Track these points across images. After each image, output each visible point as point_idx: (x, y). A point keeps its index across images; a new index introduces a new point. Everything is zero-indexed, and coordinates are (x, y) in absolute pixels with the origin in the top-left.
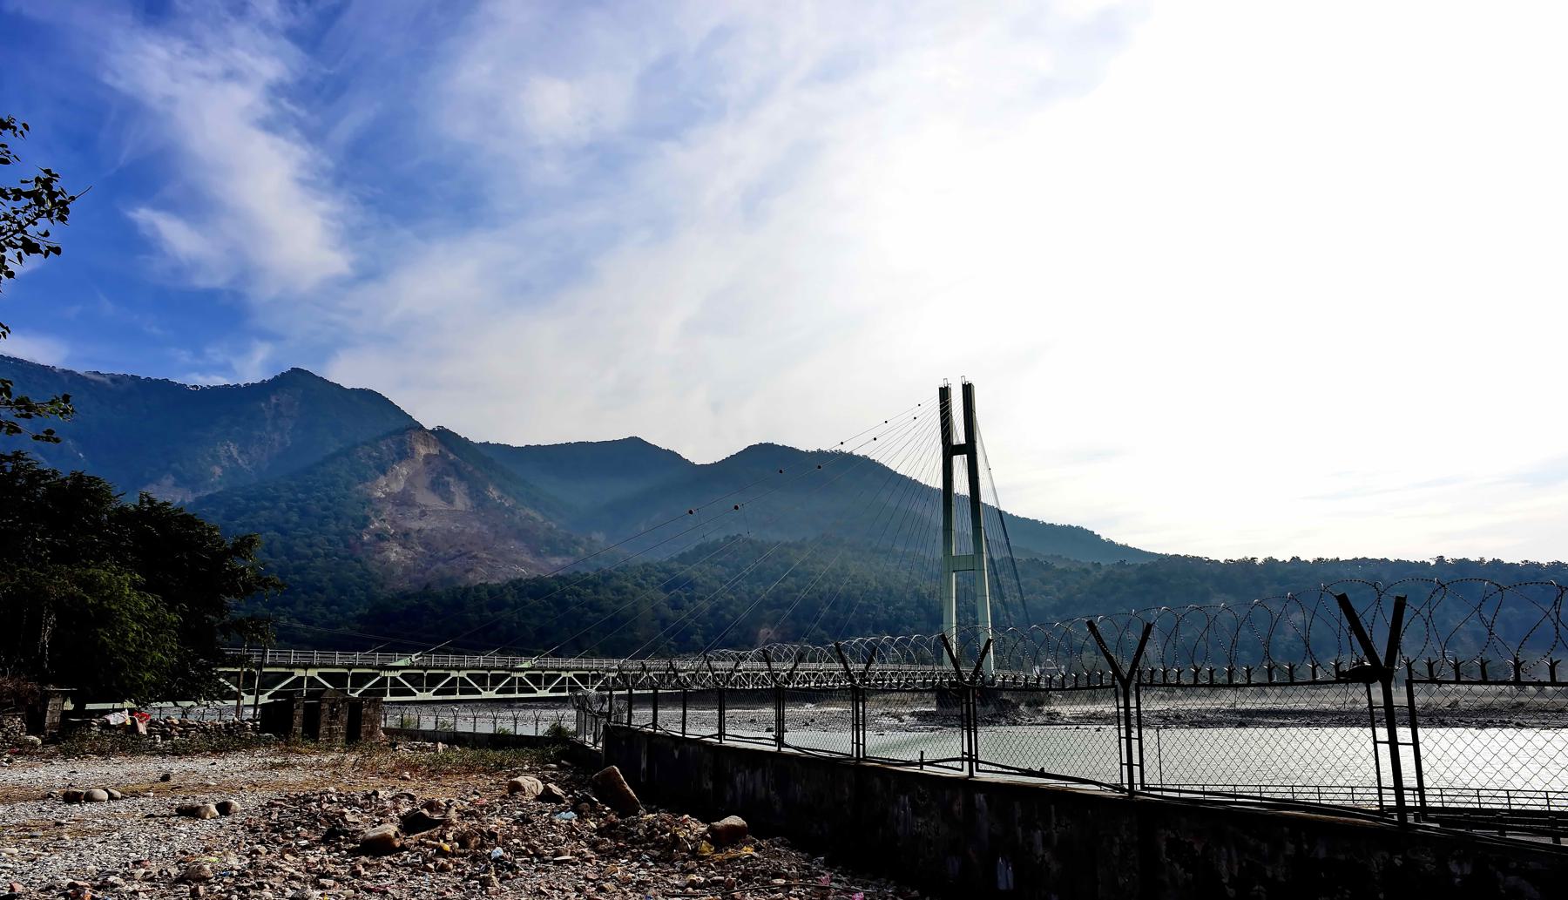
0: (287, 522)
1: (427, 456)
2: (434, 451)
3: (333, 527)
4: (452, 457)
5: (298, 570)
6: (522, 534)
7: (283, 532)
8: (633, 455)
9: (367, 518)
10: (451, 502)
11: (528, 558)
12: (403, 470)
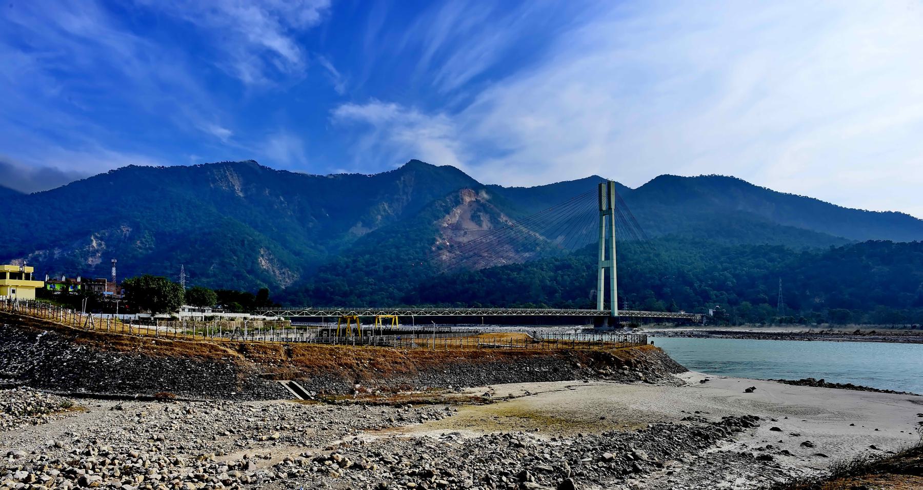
2: (474, 199)
3: (418, 245)
6: (512, 241)
8: (595, 186)
10: (480, 226)
11: (512, 254)
12: (458, 211)
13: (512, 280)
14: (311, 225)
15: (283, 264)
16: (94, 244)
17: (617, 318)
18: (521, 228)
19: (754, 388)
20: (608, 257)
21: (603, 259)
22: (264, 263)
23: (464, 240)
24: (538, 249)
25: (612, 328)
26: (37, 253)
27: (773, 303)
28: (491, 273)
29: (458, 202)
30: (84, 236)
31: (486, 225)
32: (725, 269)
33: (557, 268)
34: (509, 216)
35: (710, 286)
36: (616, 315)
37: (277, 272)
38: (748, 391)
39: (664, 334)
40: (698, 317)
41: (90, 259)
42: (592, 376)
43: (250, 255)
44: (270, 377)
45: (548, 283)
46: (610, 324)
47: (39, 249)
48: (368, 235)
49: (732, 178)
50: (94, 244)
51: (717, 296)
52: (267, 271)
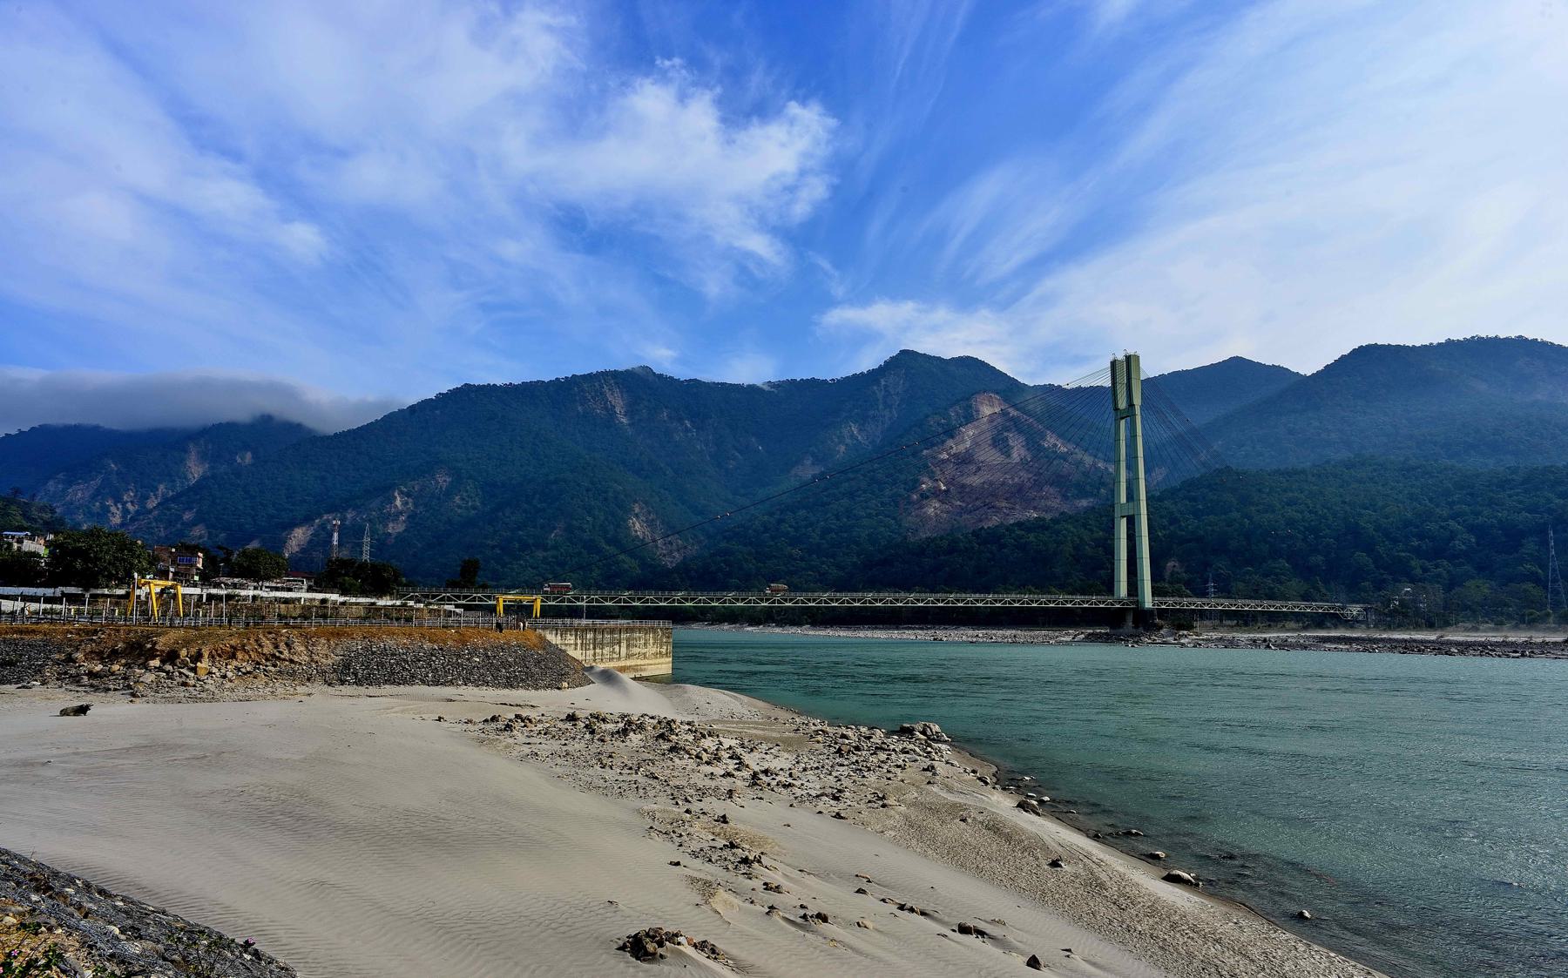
1: (992, 418)
2: (997, 410)
4: (1013, 413)
10: (1009, 456)
12: (969, 432)
14: (732, 465)
16: (398, 503)
18: (1079, 454)
23: (975, 480)
29: (970, 417)
30: (384, 491)
31: (1018, 451)
34: (1061, 436)
48: (814, 477)
49: (1521, 340)
50: (398, 503)
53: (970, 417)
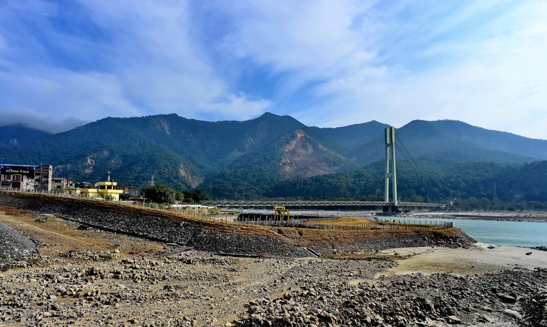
0: (261, 161)
1: (301, 137)
2: (303, 135)
4: (308, 136)
5: (262, 175)
7: (260, 164)
9: (281, 159)
10: (307, 151)
11: (326, 168)
12: (294, 142)
13: (330, 184)
14: (208, 150)
15: (193, 173)
16: (89, 161)
17: (397, 207)
19: (531, 253)
20: (391, 171)
21: (388, 172)
22: (182, 173)
23: (298, 159)
24: (342, 164)
25: (394, 212)
26: (59, 166)
27: (490, 197)
28: (316, 179)
30: (83, 157)
31: (310, 151)
32: (458, 177)
33: (356, 176)
35: (450, 187)
36: (396, 205)
37: (190, 178)
38: (527, 254)
39: (427, 216)
40: (444, 206)
41: (87, 170)
42: (435, 244)
43: (175, 168)
44: (299, 246)
45: (351, 185)
46: (393, 210)
47: (60, 164)
48: (242, 157)
50: (89, 161)
51: (454, 194)
52: (184, 177)
53: (294, 137)
